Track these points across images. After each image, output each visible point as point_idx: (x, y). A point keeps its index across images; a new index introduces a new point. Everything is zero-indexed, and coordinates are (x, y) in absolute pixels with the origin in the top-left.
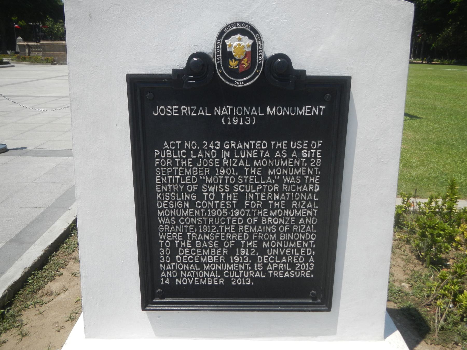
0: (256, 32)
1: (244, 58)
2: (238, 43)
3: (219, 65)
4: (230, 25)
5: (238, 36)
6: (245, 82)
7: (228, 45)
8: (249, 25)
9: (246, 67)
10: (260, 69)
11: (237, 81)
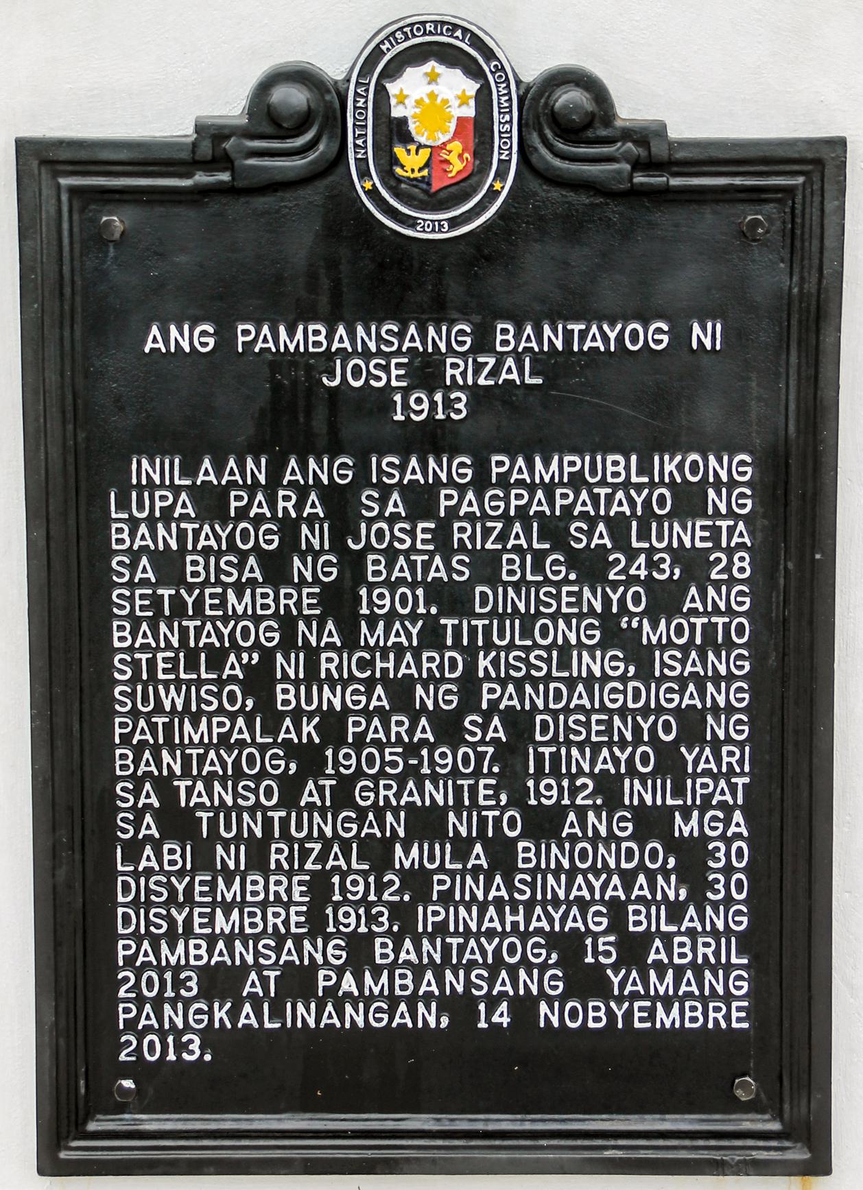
0: (489, 55)
3: (362, 163)
5: (431, 65)
6: (454, 223)
7: (395, 96)
8: (465, 30)
9: (459, 172)
10: (504, 180)
11: (424, 220)
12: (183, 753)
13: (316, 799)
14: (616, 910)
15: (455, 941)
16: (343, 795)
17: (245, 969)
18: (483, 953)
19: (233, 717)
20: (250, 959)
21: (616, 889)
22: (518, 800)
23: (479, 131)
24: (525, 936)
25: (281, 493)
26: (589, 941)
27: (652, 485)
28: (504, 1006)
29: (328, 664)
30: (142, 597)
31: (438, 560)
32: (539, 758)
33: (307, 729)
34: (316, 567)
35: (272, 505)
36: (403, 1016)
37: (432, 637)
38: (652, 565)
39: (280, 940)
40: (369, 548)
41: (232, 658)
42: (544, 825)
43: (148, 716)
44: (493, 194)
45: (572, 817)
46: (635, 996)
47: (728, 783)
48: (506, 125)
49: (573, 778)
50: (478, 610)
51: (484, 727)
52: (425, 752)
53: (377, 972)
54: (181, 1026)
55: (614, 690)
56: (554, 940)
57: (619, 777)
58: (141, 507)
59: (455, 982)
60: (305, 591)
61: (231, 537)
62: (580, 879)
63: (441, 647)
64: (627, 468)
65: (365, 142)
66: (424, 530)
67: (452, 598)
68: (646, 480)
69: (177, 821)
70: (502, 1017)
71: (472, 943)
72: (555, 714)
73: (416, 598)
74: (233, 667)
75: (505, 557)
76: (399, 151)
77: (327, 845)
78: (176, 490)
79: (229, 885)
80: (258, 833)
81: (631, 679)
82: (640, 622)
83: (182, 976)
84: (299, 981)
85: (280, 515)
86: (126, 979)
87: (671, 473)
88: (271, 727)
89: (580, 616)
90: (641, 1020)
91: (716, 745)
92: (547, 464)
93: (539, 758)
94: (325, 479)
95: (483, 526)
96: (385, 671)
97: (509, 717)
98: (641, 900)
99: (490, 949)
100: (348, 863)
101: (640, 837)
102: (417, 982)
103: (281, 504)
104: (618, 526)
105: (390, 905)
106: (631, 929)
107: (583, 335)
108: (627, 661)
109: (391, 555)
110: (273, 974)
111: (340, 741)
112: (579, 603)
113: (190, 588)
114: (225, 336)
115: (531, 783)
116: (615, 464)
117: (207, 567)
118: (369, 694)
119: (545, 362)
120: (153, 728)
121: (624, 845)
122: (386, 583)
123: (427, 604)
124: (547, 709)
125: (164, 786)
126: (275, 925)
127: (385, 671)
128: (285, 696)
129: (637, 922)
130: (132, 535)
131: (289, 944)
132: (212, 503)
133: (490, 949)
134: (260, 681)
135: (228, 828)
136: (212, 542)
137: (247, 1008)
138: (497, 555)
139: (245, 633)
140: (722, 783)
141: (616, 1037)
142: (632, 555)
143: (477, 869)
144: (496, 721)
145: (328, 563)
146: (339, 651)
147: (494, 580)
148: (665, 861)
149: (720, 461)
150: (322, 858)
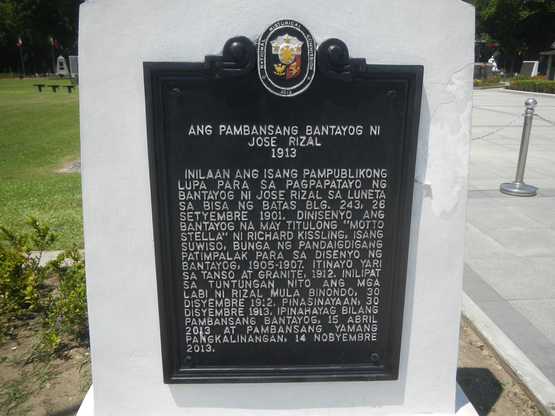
0: (307, 32)
1: (293, 63)
2: (285, 44)
3: (262, 70)
4: (276, 23)
5: (286, 36)
6: (294, 91)
7: (274, 47)
8: (299, 24)
9: (296, 74)
10: (311, 76)
12: (204, 264)
13: (246, 276)
14: (339, 308)
15: (289, 317)
16: (255, 275)
17: (224, 326)
18: (298, 321)
19: (220, 252)
20: (226, 324)
21: (338, 302)
22: (310, 276)
23: (303, 58)
24: (310, 316)
25: (235, 181)
26: (330, 317)
27: (355, 179)
28: (304, 336)
29: (250, 236)
30: (190, 215)
31: (286, 203)
32: (317, 264)
33: (243, 256)
34: (246, 205)
35: (232, 186)
36: (273, 340)
37: (283, 226)
38: (354, 204)
39: (235, 318)
40: (263, 199)
41: (219, 234)
42: (317, 283)
43: (192, 252)
44: (307, 82)
45: (326, 281)
46: (343, 332)
47: (375, 270)
48: (312, 58)
49: (327, 270)
50: (298, 218)
51: (299, 255)
52: (281, 262)
53: (265, 327)
54: (205, 342)
55: (341, 243)
56: (319, 317)
57: (341, 270)
58: (188, 186)
59: (289, 329)
60: (243, 212)
61: (218, 195)
62: (328, 300)
63: (286, 230)
64: (348, 173)
65: (264, 63)
66: (282, 193)
67: (290, 214)
68: (353, 177)
69: (202, 283)
70: (303, 339)
71: (294, 318)
72: (322, 251)
73: (278, 215)
74: (219, 237)
75: (308, 201)
76: (275, 65)
77: (249, 290)
78: (200, 180)
79: (219, 302)
80: (228, 286)
81: (346, 240)
82: (350, 222)
83: (206, 328)
84: (241, 329)
85: (234, 188)
86: (188, 329)
87: (362, 176)
88: (232, 255)
89: (331, 220)
90: (345, 339)
91: (371, 259)
92: (322, 172)
93: (317, 264)
94: (249, 176)
95: (301, 192)
96: (268, 238)
97: (308, 251)
98: (346, 305)
99: (300, 319)
100: (256, 294)
101: (346, 287)
102: (277, 330)
103: (235, 185)
104: (344, 192)
105: (269, 307)
106: (343, 313)
107: (335, 130)
108: (345, 234)
109: (270, 201)
110: (233, 327)
111: (254, 259)
112: (330, 216)
113: (205, 212)
114: (215, 129)
115: (314, 271)
116: (344, 172)
117: (210, 205)
118: (263, 245)
119: (321, 138)
120: (194, 255)
121: (342, 289)
122: (269, 210)
123: (282, 217)
124: (319, 249)
125: (198, 273)
126: (234, 314)
127: (268, 238)
128: (236, 246)
129: (344, 311)
130: (186, 195)
131: (238, 319)
132: (212, 184)
133: (300, 319)
134: (228, 240)
135: (219, 285)
136: (212, 197)
137: (225, 337)
138: (305, 201)
139: (223, 226)
140: (373, 270)
141: (337, 344)
142: (348, 201)
143: (296, 297)
144: (303, 253)
145: (250, 204)
146: (254, 232)
147: (304, 209)
148: (354, 294)
149: (377, 171)
150: (248, 294)
